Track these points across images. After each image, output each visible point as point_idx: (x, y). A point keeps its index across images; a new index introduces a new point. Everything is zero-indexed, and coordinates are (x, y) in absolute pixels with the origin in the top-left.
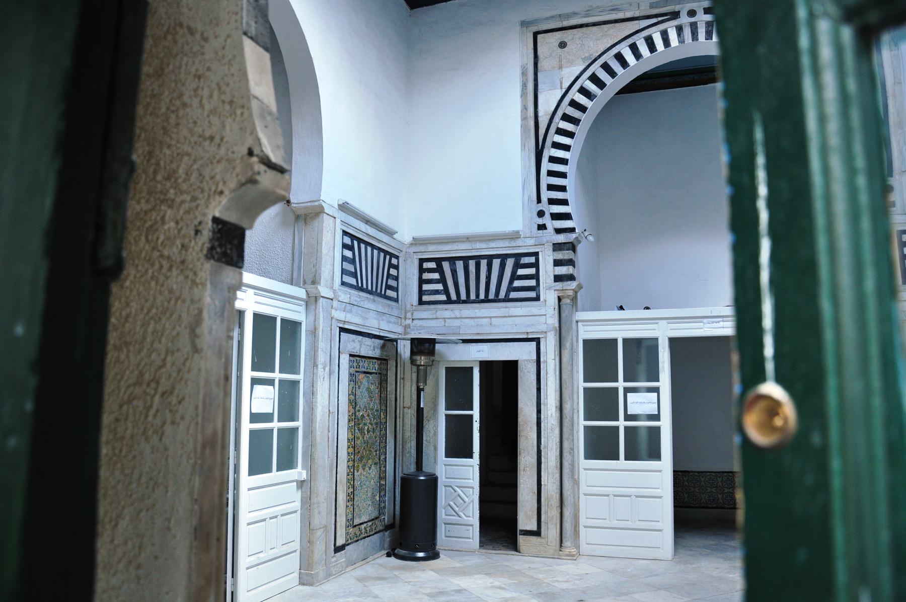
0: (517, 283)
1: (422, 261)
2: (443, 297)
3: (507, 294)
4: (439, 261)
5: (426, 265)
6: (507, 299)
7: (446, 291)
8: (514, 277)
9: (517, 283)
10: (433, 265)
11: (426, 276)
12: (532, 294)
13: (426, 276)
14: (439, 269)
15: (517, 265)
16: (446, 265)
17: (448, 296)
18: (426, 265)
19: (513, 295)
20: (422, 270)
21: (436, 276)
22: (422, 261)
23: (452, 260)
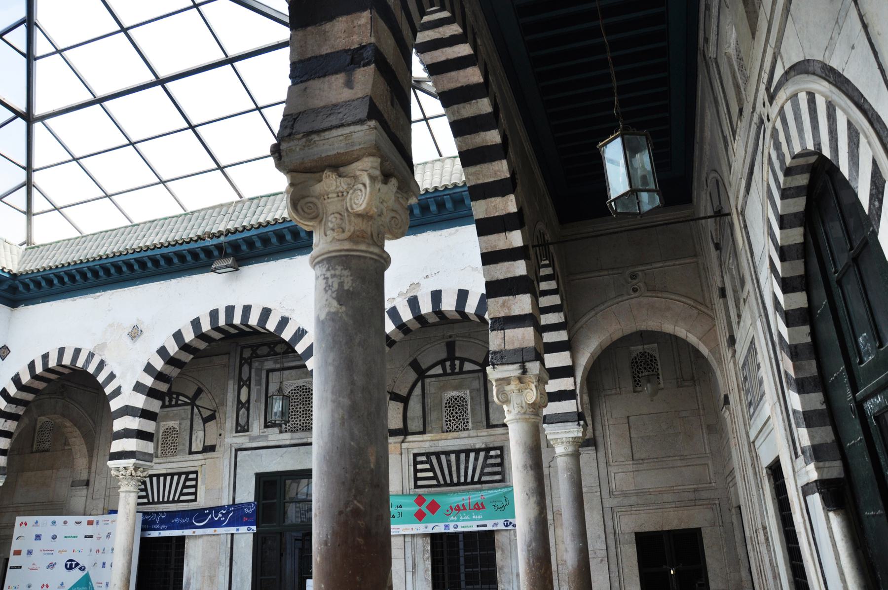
0: (185, 491)
8: (184, 487)
9: (185, 491)
12: (193, 497)
15: (187, 479)
19: (182, 498)
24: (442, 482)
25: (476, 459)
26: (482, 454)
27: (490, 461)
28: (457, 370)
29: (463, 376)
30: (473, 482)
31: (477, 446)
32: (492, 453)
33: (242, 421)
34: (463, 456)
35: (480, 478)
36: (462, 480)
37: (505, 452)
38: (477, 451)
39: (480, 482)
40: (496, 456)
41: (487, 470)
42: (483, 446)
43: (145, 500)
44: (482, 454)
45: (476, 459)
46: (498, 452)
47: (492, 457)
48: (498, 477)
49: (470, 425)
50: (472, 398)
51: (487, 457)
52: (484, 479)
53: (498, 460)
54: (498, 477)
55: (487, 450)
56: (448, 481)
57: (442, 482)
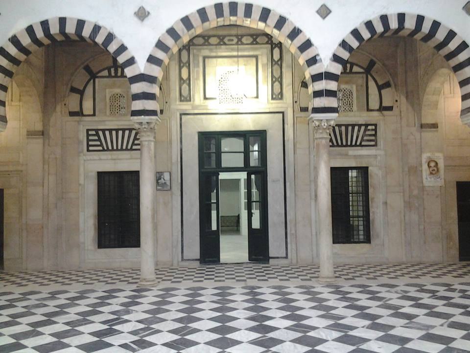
1: (88, 130)
2: (100, 148)
3: (132, 146)
4: (97, 131)
5: (90, 133)
6: (131, 149)
7: (101, 145)
10: (94, 133)
11: (91, 138)
13: (91, 138)
14: (97, 134)
16: (101, 133)
17: (103, 148)
18: (90, 133)
19: (134, 147)
20: (88, 135)
21: (96, 138)
22: (88, 130)
23: (104, 131)
24: (335, 144)
25: (359, 131)
26: (363, 128)
27: (368, 133)
28: (348, 70)
29: (352, 75)
30: (356, 145)
31: (360, 123)
32: (370, 127)
33: (185, 93)
34: (350, 128)
35: (361, 143)
36: (349, 143)
37: (378, 127)
38: (360, 126)
39: (361, 145)
40: (372, 130)
41: (365, 138)
42: (364, 123)
43: (100, 148)
44: (363, 128)
45: (359, 131)
46: (374, 127)
47: (369, 130)
48: (373, 143)
49: (355, 108)
50: (357, 91)
51: (366, 130)
52: (363, 143)
53: (373, 133)
54: (373, 143)
55: (367, 125)
56: (340, 144)
57: (335, 144)
